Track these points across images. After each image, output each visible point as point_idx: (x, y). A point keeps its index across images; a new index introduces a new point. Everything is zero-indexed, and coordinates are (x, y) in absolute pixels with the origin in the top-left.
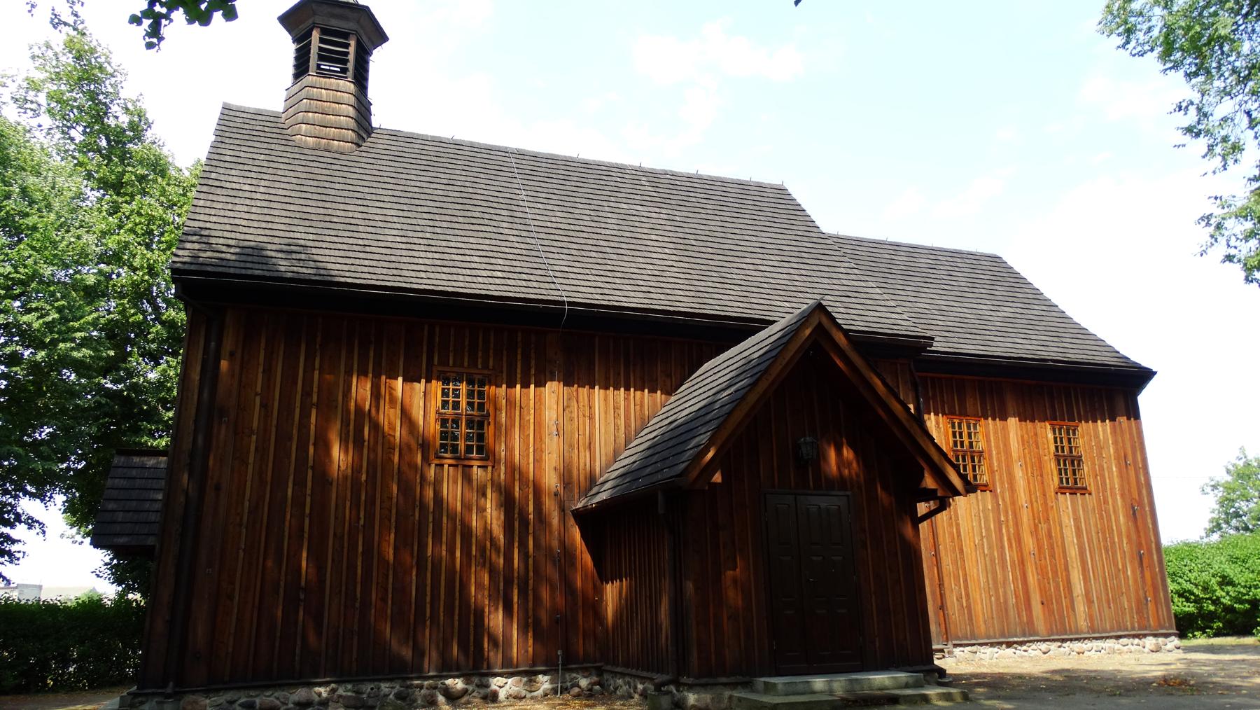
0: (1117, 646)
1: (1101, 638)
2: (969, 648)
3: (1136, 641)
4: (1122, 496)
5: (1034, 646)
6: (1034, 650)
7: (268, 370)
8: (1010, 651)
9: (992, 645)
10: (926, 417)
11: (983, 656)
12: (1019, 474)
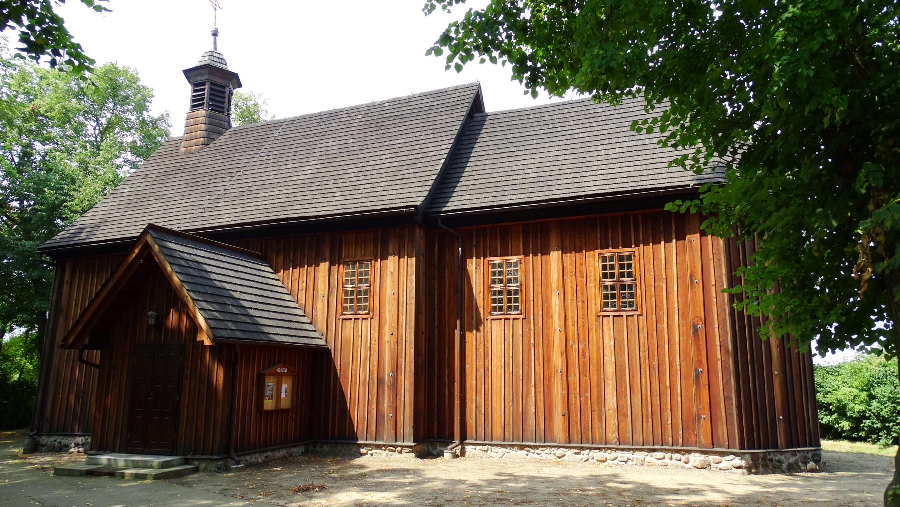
0: (649, 459)
1: (629, 450)
2: (481, 447)
3: (676, 456)
4: (683, 315)
5: (548, 451)
6: (546, 455)
7: (79, 288)
8: (523, 453)
9: (503, 446)
10: (469, 261)
11: (493, 455)
12: (556, 302)
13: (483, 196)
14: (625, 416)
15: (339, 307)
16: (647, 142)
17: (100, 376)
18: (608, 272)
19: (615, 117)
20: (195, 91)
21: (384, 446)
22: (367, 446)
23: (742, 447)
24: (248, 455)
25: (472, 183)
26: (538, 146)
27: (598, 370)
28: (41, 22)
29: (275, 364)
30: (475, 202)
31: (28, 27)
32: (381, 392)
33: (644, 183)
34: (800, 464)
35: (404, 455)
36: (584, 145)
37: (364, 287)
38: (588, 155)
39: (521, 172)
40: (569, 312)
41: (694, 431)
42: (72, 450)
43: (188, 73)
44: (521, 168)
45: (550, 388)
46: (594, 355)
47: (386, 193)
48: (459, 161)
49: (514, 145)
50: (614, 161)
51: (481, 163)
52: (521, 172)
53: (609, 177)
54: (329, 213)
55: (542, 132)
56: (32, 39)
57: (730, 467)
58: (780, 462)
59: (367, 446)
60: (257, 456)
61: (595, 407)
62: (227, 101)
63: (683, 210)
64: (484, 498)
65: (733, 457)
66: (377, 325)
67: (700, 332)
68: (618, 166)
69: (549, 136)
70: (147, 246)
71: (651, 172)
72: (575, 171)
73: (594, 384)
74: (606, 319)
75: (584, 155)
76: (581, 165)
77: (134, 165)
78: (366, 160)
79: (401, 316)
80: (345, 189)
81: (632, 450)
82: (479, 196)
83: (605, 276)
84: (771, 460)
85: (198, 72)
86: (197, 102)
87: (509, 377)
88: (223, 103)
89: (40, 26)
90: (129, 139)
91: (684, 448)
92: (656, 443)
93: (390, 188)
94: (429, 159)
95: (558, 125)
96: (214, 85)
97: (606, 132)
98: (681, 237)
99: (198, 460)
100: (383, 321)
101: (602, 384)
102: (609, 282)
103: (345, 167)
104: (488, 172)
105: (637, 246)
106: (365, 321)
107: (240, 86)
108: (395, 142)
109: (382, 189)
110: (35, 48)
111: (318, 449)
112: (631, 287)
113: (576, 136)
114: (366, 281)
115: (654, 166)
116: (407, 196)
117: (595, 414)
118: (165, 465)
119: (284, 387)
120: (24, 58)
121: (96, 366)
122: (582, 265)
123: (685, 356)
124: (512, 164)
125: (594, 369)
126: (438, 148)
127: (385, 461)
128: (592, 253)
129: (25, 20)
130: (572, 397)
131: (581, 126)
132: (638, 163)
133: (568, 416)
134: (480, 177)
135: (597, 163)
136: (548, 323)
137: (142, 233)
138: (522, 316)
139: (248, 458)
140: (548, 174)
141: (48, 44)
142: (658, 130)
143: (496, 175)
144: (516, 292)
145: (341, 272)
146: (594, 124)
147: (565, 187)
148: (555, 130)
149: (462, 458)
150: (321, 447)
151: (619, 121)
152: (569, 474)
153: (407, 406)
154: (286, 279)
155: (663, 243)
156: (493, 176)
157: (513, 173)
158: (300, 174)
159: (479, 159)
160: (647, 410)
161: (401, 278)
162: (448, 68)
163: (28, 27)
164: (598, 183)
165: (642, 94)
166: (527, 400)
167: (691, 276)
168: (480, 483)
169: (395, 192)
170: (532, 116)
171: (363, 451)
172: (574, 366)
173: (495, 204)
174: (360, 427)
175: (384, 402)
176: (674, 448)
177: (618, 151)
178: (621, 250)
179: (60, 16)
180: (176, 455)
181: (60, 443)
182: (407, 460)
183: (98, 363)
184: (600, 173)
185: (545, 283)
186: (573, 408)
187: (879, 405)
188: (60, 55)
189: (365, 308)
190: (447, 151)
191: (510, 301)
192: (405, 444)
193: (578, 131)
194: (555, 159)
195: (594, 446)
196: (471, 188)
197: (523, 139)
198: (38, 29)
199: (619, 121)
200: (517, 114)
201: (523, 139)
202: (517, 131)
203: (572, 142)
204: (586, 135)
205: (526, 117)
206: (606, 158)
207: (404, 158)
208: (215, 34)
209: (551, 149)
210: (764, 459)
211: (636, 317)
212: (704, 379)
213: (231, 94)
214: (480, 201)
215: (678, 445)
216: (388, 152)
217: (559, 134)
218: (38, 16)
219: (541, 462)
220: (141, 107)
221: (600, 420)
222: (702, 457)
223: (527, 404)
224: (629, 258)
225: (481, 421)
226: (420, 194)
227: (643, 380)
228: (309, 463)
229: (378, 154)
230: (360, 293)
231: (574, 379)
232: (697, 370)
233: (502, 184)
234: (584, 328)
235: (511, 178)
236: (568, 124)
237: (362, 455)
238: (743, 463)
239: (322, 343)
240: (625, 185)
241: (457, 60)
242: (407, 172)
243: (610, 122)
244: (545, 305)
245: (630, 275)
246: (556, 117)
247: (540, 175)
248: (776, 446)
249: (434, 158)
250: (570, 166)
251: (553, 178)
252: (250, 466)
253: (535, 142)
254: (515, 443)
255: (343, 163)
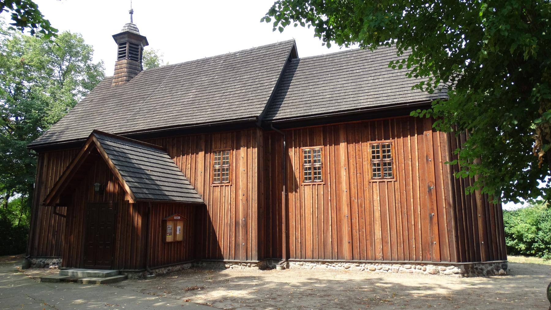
0: (401, 268)
1: (389, 263)
2: (299, 263)
4: (422, 180)
5: (339, 265)
6: (338, 267)
7: (53, 169)
9: (312, 262)
10: (290, 149)
11: (306, 267)
12: (344, 174)
13: (298, 109)
14: (387, 243)
15: (211, 179)
16: (399, 74)
17: (67, 222)
18: (376, 155)
19: (379, 59)
20: (120, 48)
21: (240, 263)
22: (229, 262)
23: (459, 261)
24: (157, 269)
25: (291, 101)
26: (332, 78)
27: (370, 215)
28: (24, 7)
29: (172, 214)
30: (293, 113)
31: (17, 11)
32: (237, 230)
33: (397, 100)
34: (495, 271)
35: (252, 268)
36: (360, 77)
37: (226, 166)
38: (362, 83)
39: (321, 94)
40: (352, 180)
41: (429, 251)
42: (51, 267)
43: (115, 37)
44: (321, 91)
45: (340, 226)
46: (367, 206)
47: (238, 109)
48: (283, 88)
49: (317, 78)
50: (379, 86)
51: (296, 89)
52: (321, 94)
53: (376, 96)
54: (204, 121)
55: (334, 69)
56: (19, 17)
57: (451, 273)
58: (482, 269)
59: (229, 262)
60: (163, 269)
61: (368, 238)
62: (139, 53)
63: (421, 116)
64: (301, 293)
65: (453, 267)
66: (234, 189)
67: (432, 191)
68: (381, 89)
69: (338, 71)
70: (93, 143)
71: (401, 93)
72: (354, 93)
73: (368, 223)
74: (374, 184)
75: (360, 83)
76: (358, 89)
77: (84, 94)
78: (226, 88)
79: (249, 184)
80: (213, 107)
81: (391, 263)
82: (295, 110)
83: (374, 157)
84: (477, 268)
85: (121, 36)
86: (121, 55)
87: (315, 220)
88: (137, 55)
89: (24, 9)
90: (80, 78)
91: (423, 262)
92: (406, 258)
93: (241, 106)
94: (264, 87)
95: (344, 65)
96: (131, 44)
97: (373, 69)
98: (420, 133)
99: (127, 272)
100: (238, 187)
101: (372, 224)
102: (376, 161)
103: (213, 93)
104: (301, 94)
105: (393, 138)
106: (227, 187)
107: (147, 44)
108: (243, 77)
109: (236, 106)
110: (21, 23)
111: (200, 265)
112: (389, 164)
113: (355, 71)
114: (227, 163)
115: (403, 89)
116: (251, 110)
117: (368, 242)
118: (108, 275)
119: (178, 228)
120: (15, 30)
121: (64, 216)
122: (359, 151)
123: (423, 206)
124: (315, 89)
125: (367, 214)
126: (270, 81)
127: (240, 272)
128: (365, 143)
129: (15, 6)
130: (354, 231)
131: (358, 65)
132: (393, 87)
133: (352, 243)
134: (296, 98)
135: (368, 88)
136: (338, 187)
137: (90, 136)
138: (323, 183)
139: (157, 271)
140: (338, 95)
141: (28, 21)
142: (405, 66)
143: (306, 97)
144: (319, 168)
145: (212, 157)
146: (366, 64)
147: (348, 103)
148: (342, 68)
149: (287, 270)
150: (202, 264)
151: (381, 61)
152: (353, 278)
153: (254, 239)
154: (178, 162)
155: (409, 136)
156: (304, 97)
157: (316, 95)
158: (186, 97)
159: (295, 86)
160: (400, 239)
161: (249, 161)
162: (274, 30)
163: (17, 11)
164: (369, 100)
165: (395, 45)
166: (326, 234)
167: (427, 156)
168: (298, 284)
169: (244, 108)
170: (327, 60)
171: (226, 266)
172: (355, 213)
173: (305, 114)
174: (225, 251)
175: (239, 236)
176: (417, 262)
177: (380, 80)
178: (383, 141)
179: (36, 3)
180: (114, 269)
181: (44, 262)
182: (254, 271)
183: (65, 214)
184: (369, 94)
185: (337, 162)
186: (354, 238)
187: (543, 234)
188: (36, 27)
189: (227, 179)
190: (275, 82)
191: (315, 173)
192: (252, 261)
193: (356, 68)
194: (342, 86)
195: (368, 261)
196: (290, 104)
197: (322, 74)
198: (22, 11)
199: (381, 61)
200: (318, 59)
201: (322, 74)
202: (318, 69)
203: (352, 75)
204: (361, 70)
205: (324, 60)
206: (373, 84)
207: (249, 87)
208: (131, 12)
209: (339, 80)
210: (472, 268)
211: (393, 182)
212: (435, 220)
213: (142, 49)
214: (296, 113)
215: (419, 260)
216: (239, 83)
217: (344, 70)
218: (22, 3)
219: (336, 271)
220: (86, 58)
221: (371, 245)
222: (434, 267)
223: (326, 236)
224: (388, 146)
225: (298, 247)
226: (259, 109)
227: (398, 221)
228: (195, 273)
229: (233, 84)
230: (223, 170)
231: (355, 220)
232: (430, 214)
233: (309, 102)
234: (361, 189)
235: (315, 98)
236: (349, 64)
237: (226, 268)
238: (459, 270)
239: (201, 200)
240: (385, 101)
241: (280, 24)
242: (251, 95)
243: (375, 62)
244: (337, 176)
245: (389, 156)
246: (342, 60)
247: (333, 96)
248: (479, 260)
249: (267, 87)
250: (352, 90)
251: (341, 97)
252: (159, 275)
253: (329, 75)
254: (319, 260)
255: (212, 91)
